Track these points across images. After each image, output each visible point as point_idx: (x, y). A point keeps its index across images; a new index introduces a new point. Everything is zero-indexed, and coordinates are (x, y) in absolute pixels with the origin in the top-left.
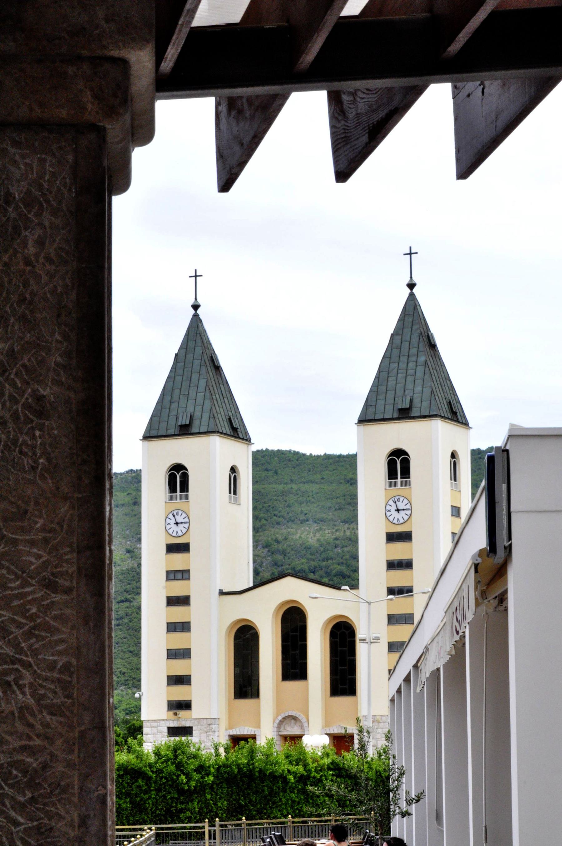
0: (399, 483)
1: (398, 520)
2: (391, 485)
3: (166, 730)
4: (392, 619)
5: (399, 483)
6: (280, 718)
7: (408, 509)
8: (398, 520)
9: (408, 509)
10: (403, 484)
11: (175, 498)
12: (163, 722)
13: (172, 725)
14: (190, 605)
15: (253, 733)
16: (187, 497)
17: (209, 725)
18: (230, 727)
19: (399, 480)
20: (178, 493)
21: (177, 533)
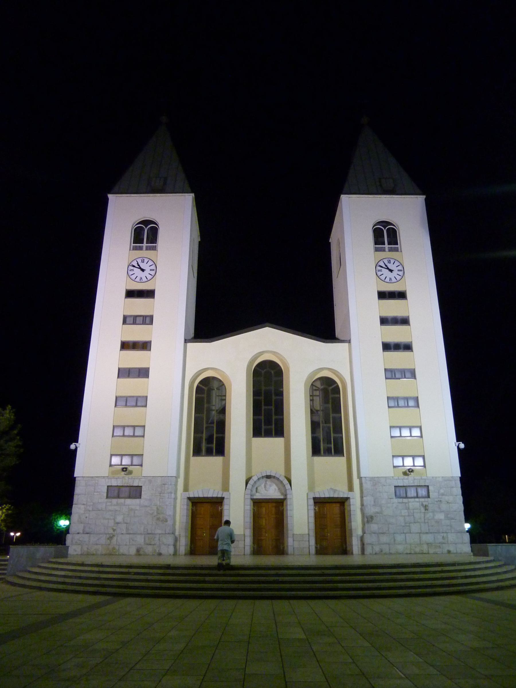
0: (387, 249)
1: (390, 279)
2: (376, 250)
3: (105, 489)
4: (391, 374)
5: (387, 249)
6: (255, 478)
7: (401, 271)
8: (390, 279)
9: (401, 271)
10: (391, 250)
11: (141, 248)
12: (103, 480)
13: (114, 484)
14: (150, 350)
15: (220, 496)
16: (154, 249)
17: (164, 484)
18: (186, 489)
19: (386, 246)
20: (145, 245)
21: (141, 278)
